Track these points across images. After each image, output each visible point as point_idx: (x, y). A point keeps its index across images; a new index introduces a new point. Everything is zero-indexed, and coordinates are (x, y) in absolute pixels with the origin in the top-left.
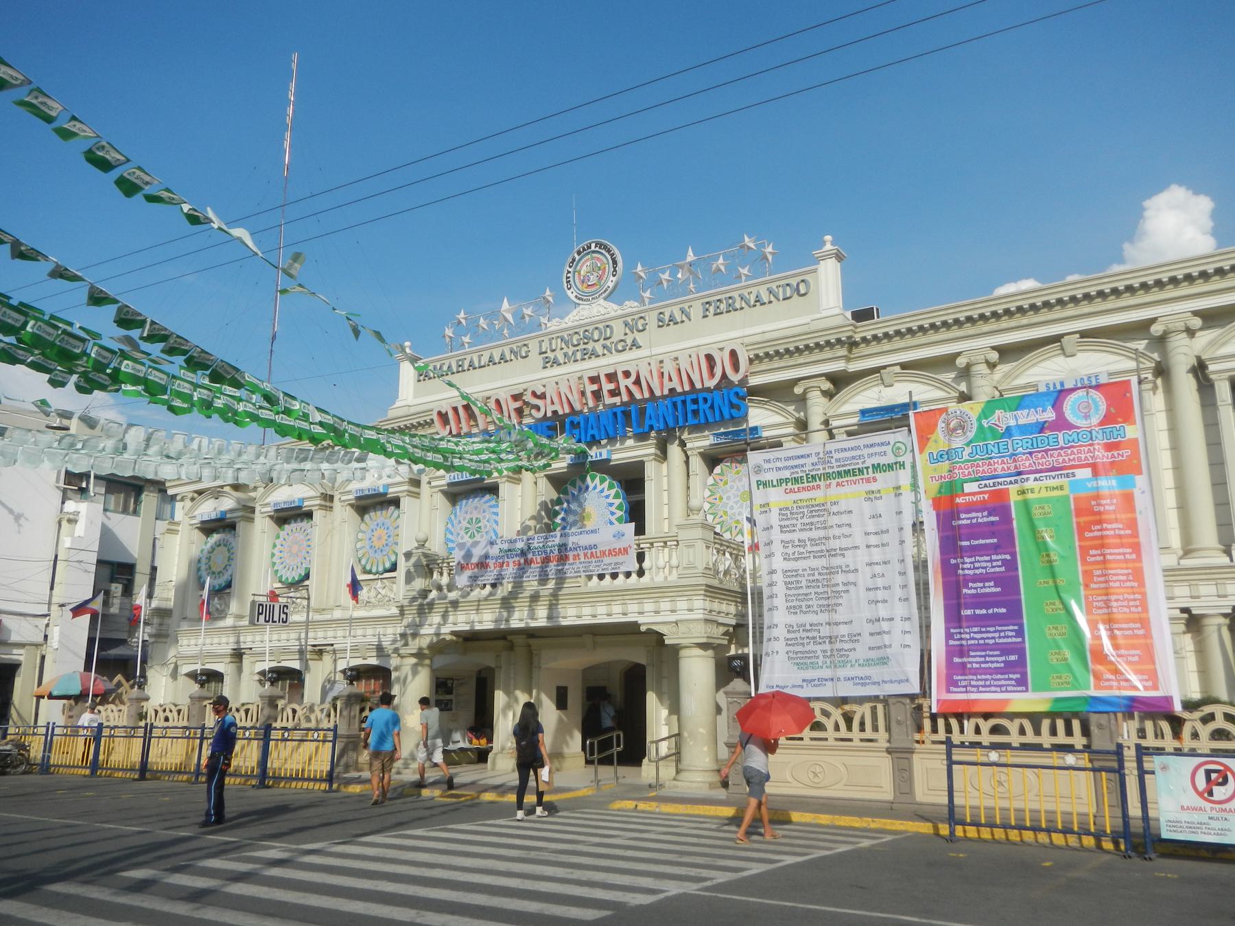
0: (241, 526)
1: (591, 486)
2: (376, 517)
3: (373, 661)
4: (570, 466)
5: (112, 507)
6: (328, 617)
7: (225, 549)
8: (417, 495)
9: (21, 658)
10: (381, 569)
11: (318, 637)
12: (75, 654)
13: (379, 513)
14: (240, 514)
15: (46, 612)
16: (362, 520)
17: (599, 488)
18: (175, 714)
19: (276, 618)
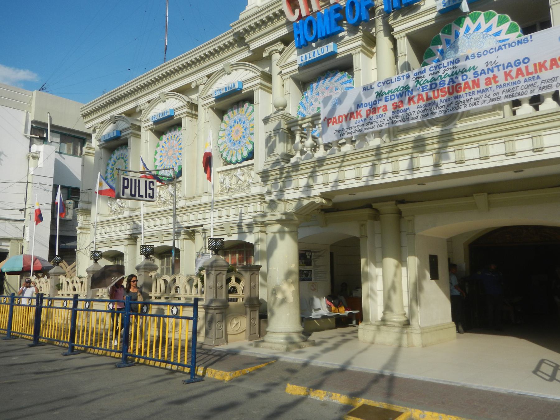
0: (132, 142)
1: (473, 27)
2: (233, 115)
3: (235, 237)
4: (436, 18)
5: (65, 151)
6: (197, 202)
7: (123, 161)
8: (269, 90)
9: (8, 248)
10: (240, 158)
11: (187, 220)
12: (43, 245)
13: (235, 111)
14: (130, 131)
15: (23, 218)
16: (222, 120)
17: (484, 27)
18: (79, 284)
19: (143, 193)
